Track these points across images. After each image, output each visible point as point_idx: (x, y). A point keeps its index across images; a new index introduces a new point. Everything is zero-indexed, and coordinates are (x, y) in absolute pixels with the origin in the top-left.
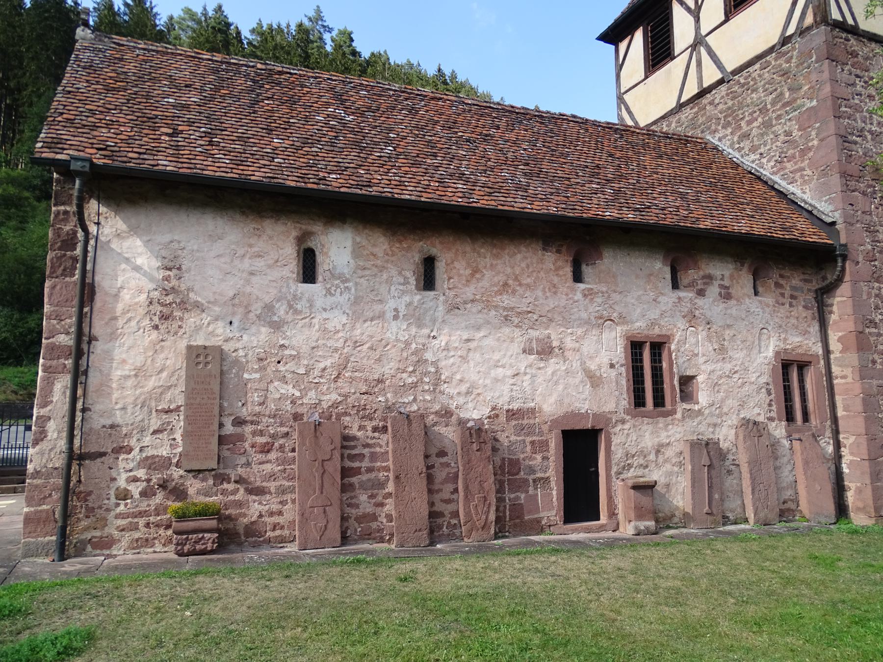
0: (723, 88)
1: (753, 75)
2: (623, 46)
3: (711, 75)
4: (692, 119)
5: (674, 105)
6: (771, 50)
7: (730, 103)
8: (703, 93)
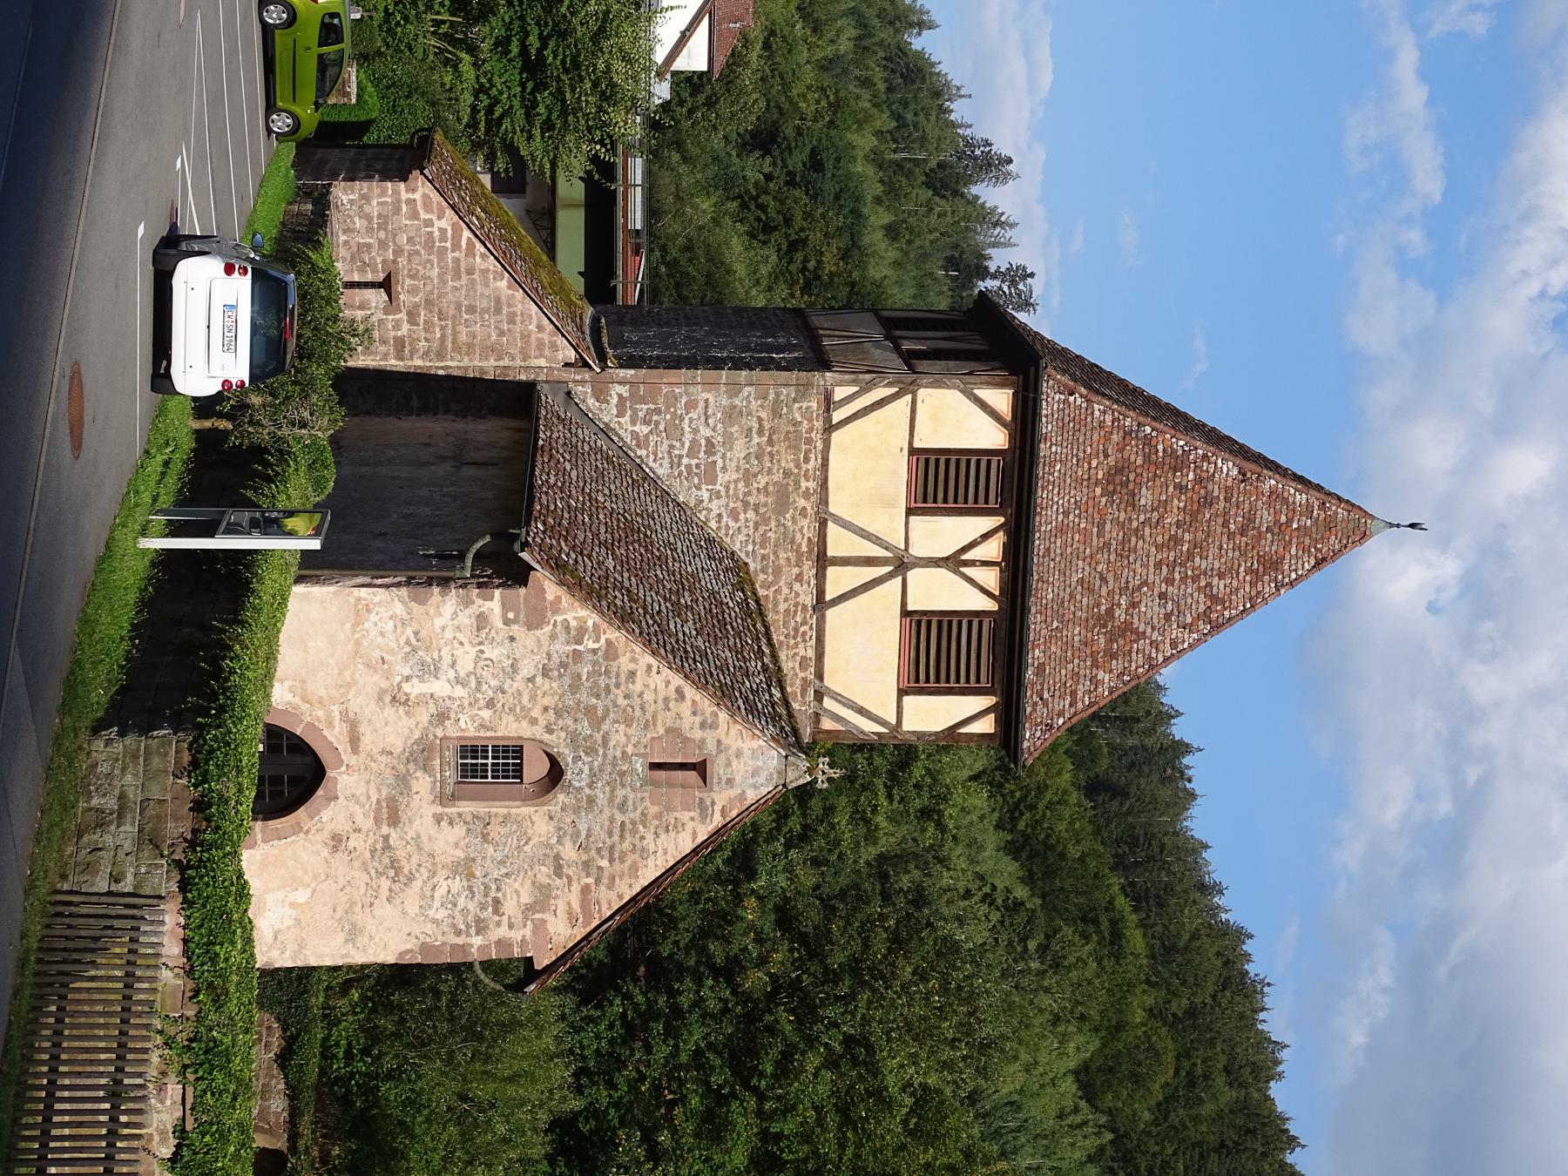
0: (809, 599)
1: (801, 645)
2: (1001, 399)
3: (839, 580)
4: (793, 541)
5: (832, 509)
6: (820, 676)
7: (782, 607)
8: (823, 561)
